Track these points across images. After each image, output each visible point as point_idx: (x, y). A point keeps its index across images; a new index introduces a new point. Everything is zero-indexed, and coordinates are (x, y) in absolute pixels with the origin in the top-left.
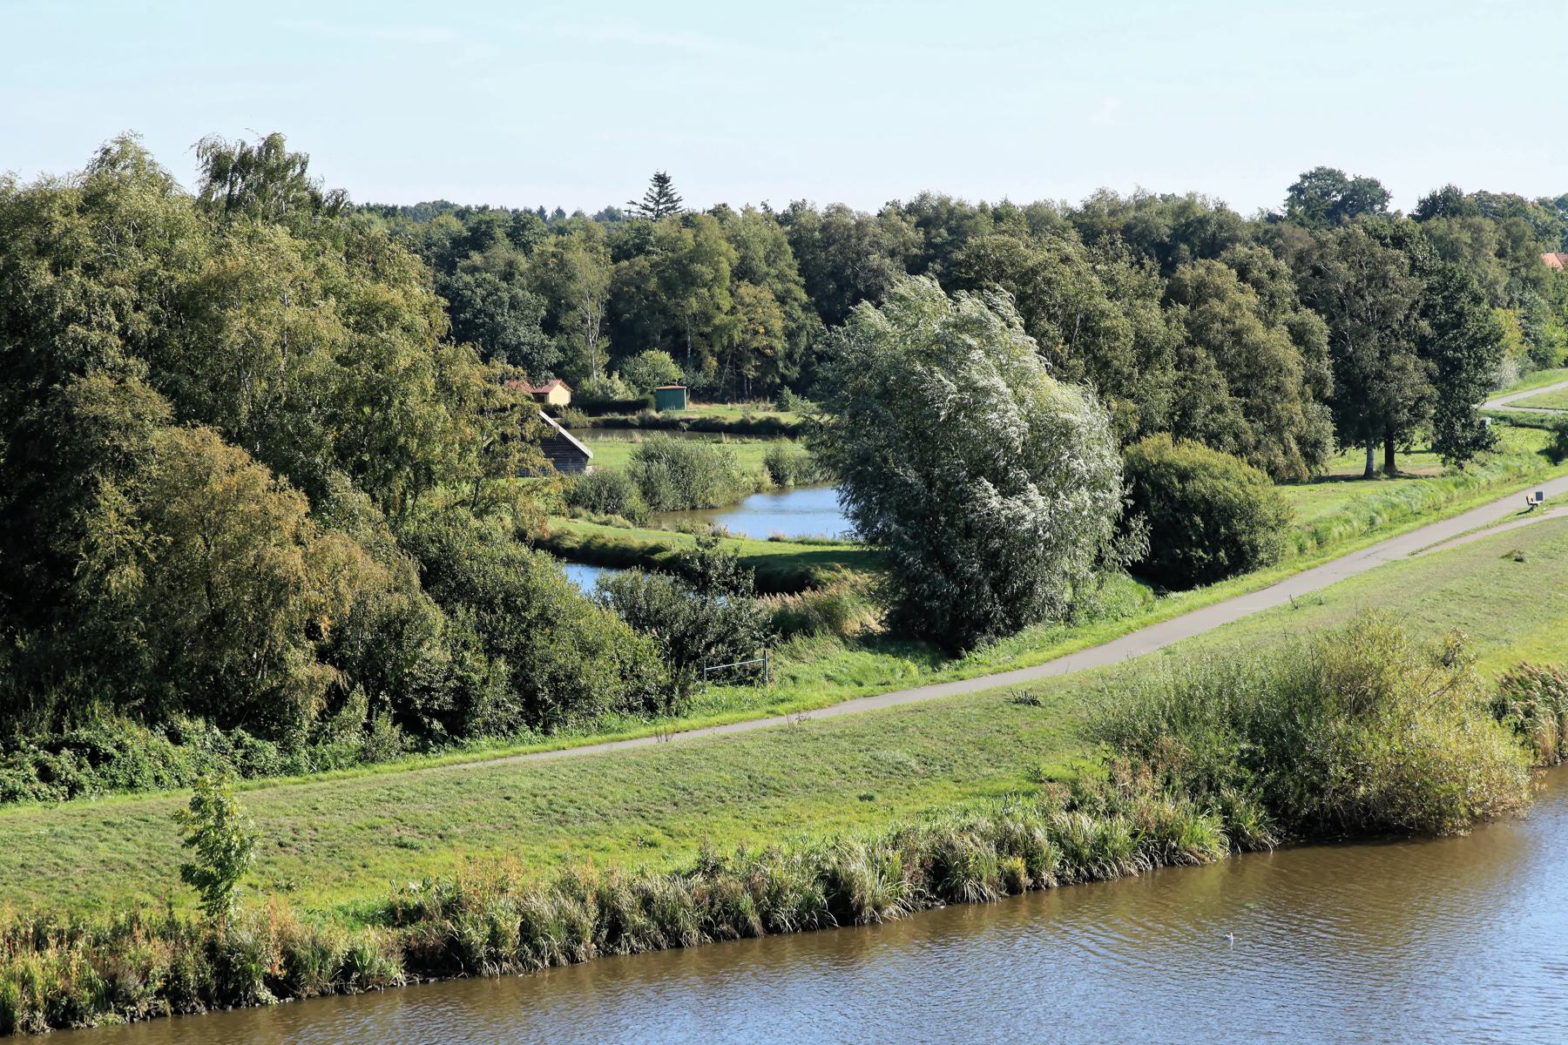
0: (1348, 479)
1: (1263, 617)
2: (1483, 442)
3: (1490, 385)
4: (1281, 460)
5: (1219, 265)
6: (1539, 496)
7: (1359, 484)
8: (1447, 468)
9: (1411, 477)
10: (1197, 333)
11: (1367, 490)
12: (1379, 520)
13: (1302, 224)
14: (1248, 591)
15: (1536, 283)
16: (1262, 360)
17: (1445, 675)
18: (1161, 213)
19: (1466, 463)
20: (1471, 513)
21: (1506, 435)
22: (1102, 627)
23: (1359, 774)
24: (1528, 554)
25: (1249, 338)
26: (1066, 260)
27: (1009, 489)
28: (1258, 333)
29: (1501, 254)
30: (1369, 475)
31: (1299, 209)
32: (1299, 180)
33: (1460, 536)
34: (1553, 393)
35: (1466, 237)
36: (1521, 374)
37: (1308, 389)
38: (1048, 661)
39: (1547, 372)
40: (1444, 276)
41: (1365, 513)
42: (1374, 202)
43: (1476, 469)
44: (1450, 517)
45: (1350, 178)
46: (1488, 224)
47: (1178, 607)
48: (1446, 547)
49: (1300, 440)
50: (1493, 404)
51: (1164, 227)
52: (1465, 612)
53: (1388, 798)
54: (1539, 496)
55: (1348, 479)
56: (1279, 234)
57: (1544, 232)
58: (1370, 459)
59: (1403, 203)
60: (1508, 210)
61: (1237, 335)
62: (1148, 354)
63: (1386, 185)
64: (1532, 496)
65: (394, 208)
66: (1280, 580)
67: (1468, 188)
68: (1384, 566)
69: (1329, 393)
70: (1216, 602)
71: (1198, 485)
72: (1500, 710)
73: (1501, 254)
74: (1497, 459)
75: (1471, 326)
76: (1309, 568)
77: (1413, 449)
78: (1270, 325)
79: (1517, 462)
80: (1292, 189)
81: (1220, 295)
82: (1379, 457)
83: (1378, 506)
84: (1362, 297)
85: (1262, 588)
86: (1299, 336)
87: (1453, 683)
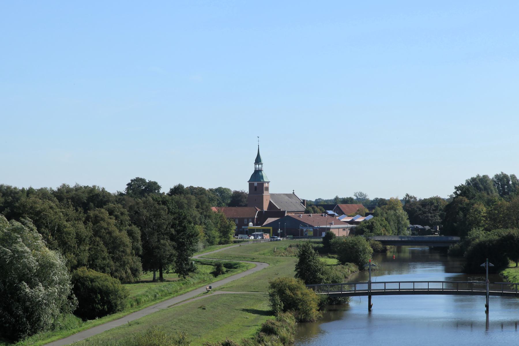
0: (147, 282)
1: (119, 328)
2: (192, 269)
3: (194, 251)
4: (124, 275)
5: (103, 210)
6: (210, 288)
7: (151, 283)
8: (180, 278)
10: (96, 233)
11: (153, 286)
12: (158, 296)
13: (131, 196)
14: (114, 320)
15: (209, 217)
16: (118, 241)
18: (83, 192)
19: (187, 277)
20: (188, 293)
22: (65, 332)
24: (207, 307)
25: (114, 235)
26: (51, 208)
27: (32, 286)
28: (117, 233)
30: (154, 281)
31: (130, 191)
32: (130, 182)
36: (204, 247)
37: (134, 252)
38: (46, 344)
39: (213, 246)
40: (179, 214)
41: (153, 293)
42: (155, 189)
44: (181, 295)
45: (147, 181)
46: (193, 197)
47: (90, 325)
48: (180, 305)
49: (131, 269)
50: (195, 257)
51: (85, 197)
52: (186, 327)
54: (210, 288)
55: (147, 282)
56: (124, 200)
57: (211, 200)
59: (165, 189)
60: (199, 192)
61: (110, 233)
62: (80, 240)
63: (159, 184)
64: (208, 288)
66: (125, 316)
67: (186, 185)
68: (159, 311)
69: (141, 253)
70: (103, 323)
71: (97, 284)
73: (197, 207)
74: (197, 275)
75: (188, 232)
76: (134, 312)
77: (169, 272)
78: (120, 231)
79: (203, 276)
80: (128, 185)
81: (103, 219)
82: (158, 274)
83: (157, 291)
84: (152, 221)
85: (119, 319)
86: (130, 234)
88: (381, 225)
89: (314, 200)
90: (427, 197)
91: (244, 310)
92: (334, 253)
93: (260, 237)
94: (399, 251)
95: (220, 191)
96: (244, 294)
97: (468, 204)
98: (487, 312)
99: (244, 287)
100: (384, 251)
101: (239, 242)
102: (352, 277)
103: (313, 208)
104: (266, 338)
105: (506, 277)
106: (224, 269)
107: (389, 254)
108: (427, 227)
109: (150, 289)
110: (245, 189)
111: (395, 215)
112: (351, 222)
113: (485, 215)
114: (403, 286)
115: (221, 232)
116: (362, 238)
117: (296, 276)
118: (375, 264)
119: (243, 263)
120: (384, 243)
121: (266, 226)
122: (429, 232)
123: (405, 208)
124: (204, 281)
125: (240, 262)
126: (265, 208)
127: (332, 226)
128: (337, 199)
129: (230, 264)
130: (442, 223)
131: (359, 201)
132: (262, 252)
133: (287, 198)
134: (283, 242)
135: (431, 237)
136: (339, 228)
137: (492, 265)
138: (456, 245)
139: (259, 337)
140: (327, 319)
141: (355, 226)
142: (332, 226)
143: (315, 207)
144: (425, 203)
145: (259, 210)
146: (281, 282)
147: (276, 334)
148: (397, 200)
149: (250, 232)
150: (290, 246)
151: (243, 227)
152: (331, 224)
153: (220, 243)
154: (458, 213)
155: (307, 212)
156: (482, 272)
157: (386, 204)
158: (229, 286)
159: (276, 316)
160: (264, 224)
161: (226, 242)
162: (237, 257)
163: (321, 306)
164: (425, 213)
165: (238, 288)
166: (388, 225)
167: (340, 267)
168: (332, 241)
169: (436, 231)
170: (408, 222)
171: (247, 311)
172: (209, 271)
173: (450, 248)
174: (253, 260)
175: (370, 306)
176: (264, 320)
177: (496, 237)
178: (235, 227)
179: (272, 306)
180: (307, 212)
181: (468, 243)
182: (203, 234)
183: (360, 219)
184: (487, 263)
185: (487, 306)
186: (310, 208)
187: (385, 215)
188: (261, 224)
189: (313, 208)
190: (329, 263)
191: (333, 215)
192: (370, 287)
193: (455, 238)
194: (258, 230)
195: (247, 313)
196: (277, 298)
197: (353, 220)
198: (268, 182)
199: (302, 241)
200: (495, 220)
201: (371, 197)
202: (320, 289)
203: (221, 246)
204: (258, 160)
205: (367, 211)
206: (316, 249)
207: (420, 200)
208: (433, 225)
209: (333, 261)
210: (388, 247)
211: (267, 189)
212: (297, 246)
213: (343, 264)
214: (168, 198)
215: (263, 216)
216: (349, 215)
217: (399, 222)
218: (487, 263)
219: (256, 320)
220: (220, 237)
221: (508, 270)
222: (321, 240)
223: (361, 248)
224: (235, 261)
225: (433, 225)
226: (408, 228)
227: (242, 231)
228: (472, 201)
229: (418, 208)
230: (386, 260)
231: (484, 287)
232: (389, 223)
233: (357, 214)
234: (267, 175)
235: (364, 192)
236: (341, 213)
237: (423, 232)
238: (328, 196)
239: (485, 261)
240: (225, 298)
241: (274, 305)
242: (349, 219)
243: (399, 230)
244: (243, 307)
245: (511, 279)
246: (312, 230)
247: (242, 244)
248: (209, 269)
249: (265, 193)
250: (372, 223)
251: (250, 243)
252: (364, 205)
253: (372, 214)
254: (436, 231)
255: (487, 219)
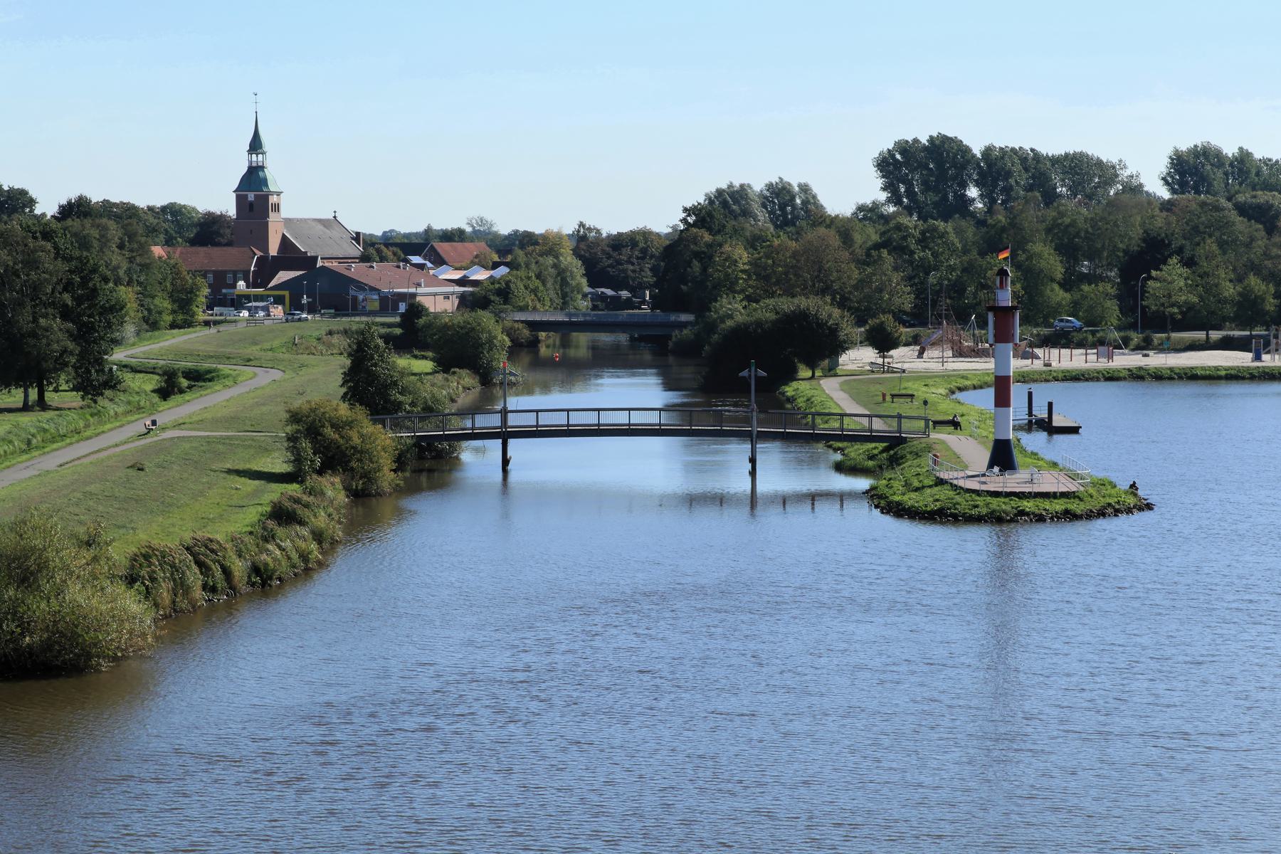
0: (10, 410)
2: (112, 383)
3: (116, 342)
6: (154, 423)
7: (19, 414)
9: (57, 409)
11: (25, 419)
12: (34, 441)
15: (145, 267)
17: (88, 554)
19: (99, 399)
21: (130, 380)
23: (25, 628)
24: (147, 465)
29: (121, 246)
30: (26, 408)
33: (98, 451)
34: (161, 348)
35: (95, 233)
36: (138, 333)
39: (156, 333)
42: (24, 206)
43: (106, 403)
45: (6, 188)
46: (112, 224)
48: (86, 461)
50: (119, 355)
52: (101, 508)
53: (47, 646)
54: (154, 423)
55: (10, 410)
57: (152, 231)
58: (26, 396)
59: (47, 207)
60: (125, 214)
63: (33, 193)
64: (148, 422)
65: (1049, 493)
67: (96, 197)
68: (39, 475)
72: (131, 580)
73: (121, 247)
74: (122, 397)
75: (101, 300)
77: (61, 388)
82: (33, 394)
83: (33, 430)
84: (19, 277)
87: (95, 559)
88: (526, 288)
89: (379, 233)
90: (625, 227)
91: (230, 472)
92: (424, 346)
93: (262, 314)
94: (565, 344)
95: (173, 211)
96: (228, 438)
97: (709, 246)
98: (753, 473)
99: (230, 421)
100: (534, 344)
101: (216, 323)
102: (465, 400)
103: (379, 251)
104: (280, 531)
105: (791, 400)
106: (184, 383)
107: (543, 350)
108: (625, 294)
109: (17, 426)
110: (227, 206)
111: (555, 266)
112: (462, 282)
113: (747, 267)
114: (577, 419)
115: (174, 301)
116: (486, 318)
117: (344, 397)
118: (516, 371)
119: (225, 369)
120: (534, 326)
121: (277, 287)
122: (628, 304)
123: (576, 252)
124: (139, 409)
125: (219, 366)
126: (273, 250)
127: (420, 290)
128: (428, 231)
129: (197, 371)
130: (656, 285)
131: (477, 235)
132: (267, 346)
133: (321, 227)
134: (314, 324)
135: (634, 315)
136: (435, 295)
137: (762, 373)
138: (685, 332)
139: (265, 529)
140: (412, 489)
141: (470, 289)
142: (420, 290)
143: (382, 247)
144: (619, 243)
145: (259, 253)
146: (313, 410)
147: (301, 523)
148: (559, 236)
149: (238, 303)
150: (330, 333)
151: (224, 291)
152: (419, 285)
153: (173, 326)
154: (689, 264)
155: (365, 258)
156: (740, 388)
157: (536, 243)
158: (195, 418)
159: (301, 482)
160: (272, 284)
161: (188, 324)
162: (212, 357)
163: (400, 463)
164: (622, 264)
165: (216, 423)
166: (541, 288)
167: (440, 376)
168: (422, 321)
169: (644, 302)
170: (584, 281)
171: (240, 473)
172: (149, 387)
173: (674, 339)
174: (248, 361)
175: (506, 462)
176: (275, 492)
177: (771, 316)
178: (206, 291)
179: (293, 462)
180: (365, 258)
181: (711, 327)
182: (135, 305)
183: (480, 275)
184: (753, 369)
185: (753, 461)
186: (372, 251)
187: (533, 266)
188: (264, 285)
189: (379, 251)
190: (416, 370)
191: (421, 267)
192: (504, 420)
193: (684, 317)
194: (258, 298)
195: (237, 478)
196: (306, 445)
197: (465, 276)
198: (279, 194)
199: (356, 322)
200: (767, 278)
201: (504, 229)
202: (397, 426)
203: (175, 331)
204: (256, 145)
205: (496, 258)
206: (387, 338)
207: (609, 236)
208: (636, 289)
209: (425, 366)
210: (542, 335)
211: (277, 208)
212: (346, 332)
213: (446, 371)
214: (55, 225)
215: (268, 268)
216: (458, 265)
217: (564, 283)
218: (753, 369)
219: (256, 493)
220: (174, 312)
221: (795, 384)
222: (398, 319)
223: (484, 336)
224: (206, 365)
225: (636, 289)
226: (585, 296)
227: (223, 298)
228: (719, 238)
229: (603, 251)
230: (539, 363)
231: (747, 421)
232: (544, 283)
233: (473, 263)
234: (276, 176)
235: (489, 217)
236: (439, 261)
237: (616, 303)
238: (410, 224)
239: (748, 366)
240: (187, 446)
241: (298, 460)
242: (457, 275)
243: (565, 300)
244: (229, 466)
245: (801, 402)
246: (376, 297)
247: (222, 328)
248: (149, 383)
249: (272, 217)
250: (508, 283)
251: (241, 326)
252: (490, 246)
253: (506, 264)
254: (644, 302)
255: (750, 277)
